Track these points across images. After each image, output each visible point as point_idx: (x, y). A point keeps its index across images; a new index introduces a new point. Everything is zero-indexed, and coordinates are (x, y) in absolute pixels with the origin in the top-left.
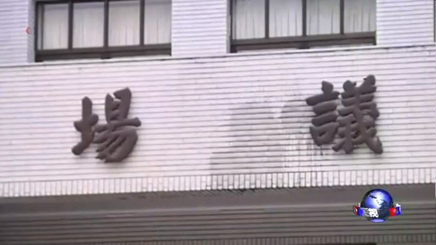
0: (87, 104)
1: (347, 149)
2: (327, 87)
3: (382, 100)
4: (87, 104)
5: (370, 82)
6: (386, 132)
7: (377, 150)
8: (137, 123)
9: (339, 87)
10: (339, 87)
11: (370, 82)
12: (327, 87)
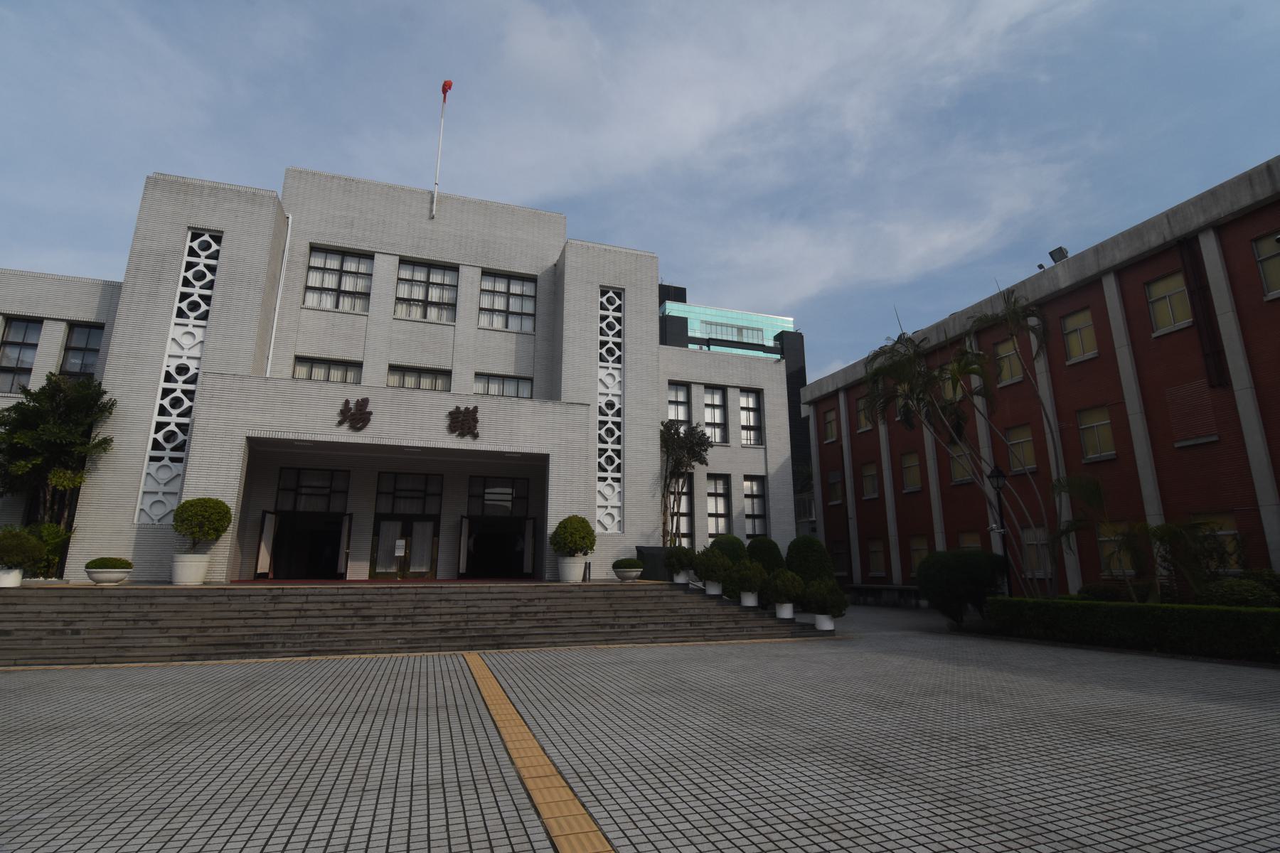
0: (347, 402)
1: (462, 435)
2: (458, 408)
3: (479, 416)
4: (347, 402)
5: (476, 408)
6: (479, 429)
7: (475, 436)
8: (371, 413)
9: (462, 409)
10: (462, 409)
11: (476, 408)
12: (458, 408)
